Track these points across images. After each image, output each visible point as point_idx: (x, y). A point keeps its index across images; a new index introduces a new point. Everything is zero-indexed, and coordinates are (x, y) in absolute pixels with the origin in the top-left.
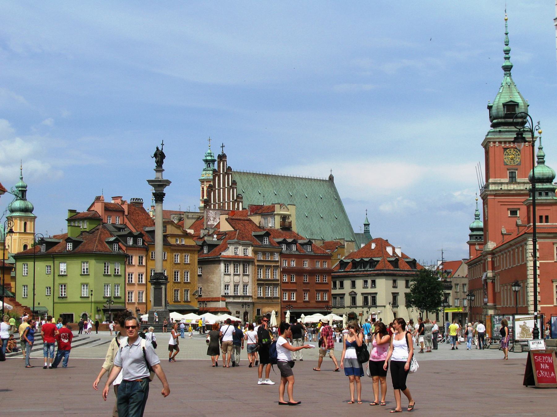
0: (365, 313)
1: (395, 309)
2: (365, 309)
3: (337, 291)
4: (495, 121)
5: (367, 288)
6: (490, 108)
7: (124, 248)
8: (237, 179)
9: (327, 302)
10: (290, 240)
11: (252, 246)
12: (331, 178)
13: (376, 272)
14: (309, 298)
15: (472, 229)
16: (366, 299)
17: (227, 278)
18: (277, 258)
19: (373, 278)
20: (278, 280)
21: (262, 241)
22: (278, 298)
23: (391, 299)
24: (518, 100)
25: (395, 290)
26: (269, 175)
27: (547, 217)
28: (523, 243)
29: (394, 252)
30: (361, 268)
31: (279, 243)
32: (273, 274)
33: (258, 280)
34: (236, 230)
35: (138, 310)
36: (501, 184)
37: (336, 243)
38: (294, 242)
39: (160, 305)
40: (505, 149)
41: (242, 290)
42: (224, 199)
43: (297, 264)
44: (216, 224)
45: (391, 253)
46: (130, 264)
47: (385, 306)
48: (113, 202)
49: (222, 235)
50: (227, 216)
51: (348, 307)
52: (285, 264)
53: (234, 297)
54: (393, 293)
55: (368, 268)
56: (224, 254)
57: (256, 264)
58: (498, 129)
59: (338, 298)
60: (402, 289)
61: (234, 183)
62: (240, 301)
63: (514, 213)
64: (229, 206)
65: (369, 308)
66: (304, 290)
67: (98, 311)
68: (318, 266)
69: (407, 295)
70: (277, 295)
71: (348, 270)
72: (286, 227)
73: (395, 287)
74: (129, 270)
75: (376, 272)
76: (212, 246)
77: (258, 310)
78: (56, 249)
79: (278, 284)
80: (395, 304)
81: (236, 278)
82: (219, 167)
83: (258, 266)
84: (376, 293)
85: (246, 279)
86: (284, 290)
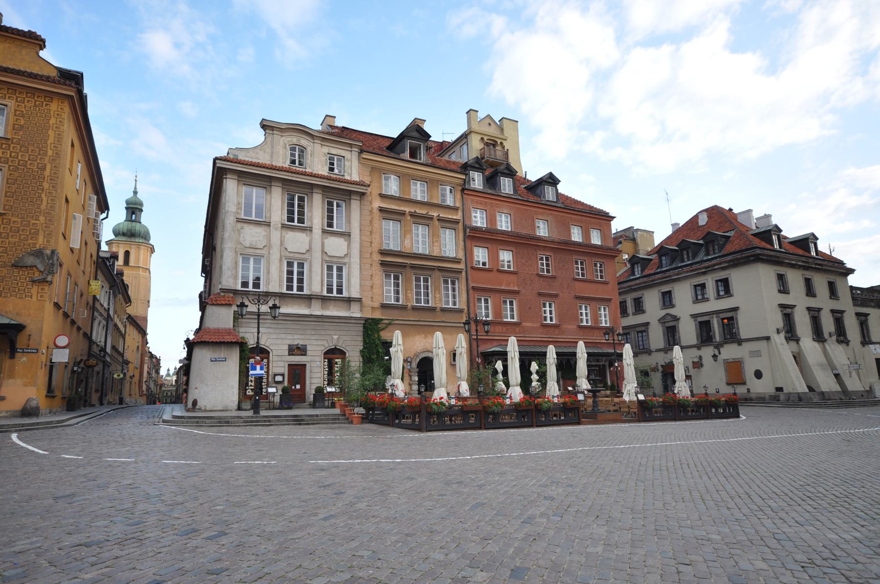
0: (707, 359)
1: (793, 344)
2: (707, 352)
5: (707, 300)
11: (361, 151)
13: (729, 258)
14: (560, 316)
17: (252, 235)
19: (722, 275)
20: (456, 261)
22: (460, 311)
23: (780, 324)
30: (683, 261)
32: (435, 237)
33: (383, 253)
41: (316, 279)
43: (514, 222)
47: (768, 338)
51: (658, 350)
52: (479, 219)
54: (782, 306)
55: (701, 256)
57: (377, 203)
62: (306, 311)
65: (718, 346)
66: (540, 294)
68: (576, 236)
69: (815, 315)
70: (461, 304)
71: (652, 272)
73: (780, 291)
75: (729, 258)
79: (459, 272)
83: (382, 210)
84: (735, 309)
85: (336, 246)
86: (473, 288)
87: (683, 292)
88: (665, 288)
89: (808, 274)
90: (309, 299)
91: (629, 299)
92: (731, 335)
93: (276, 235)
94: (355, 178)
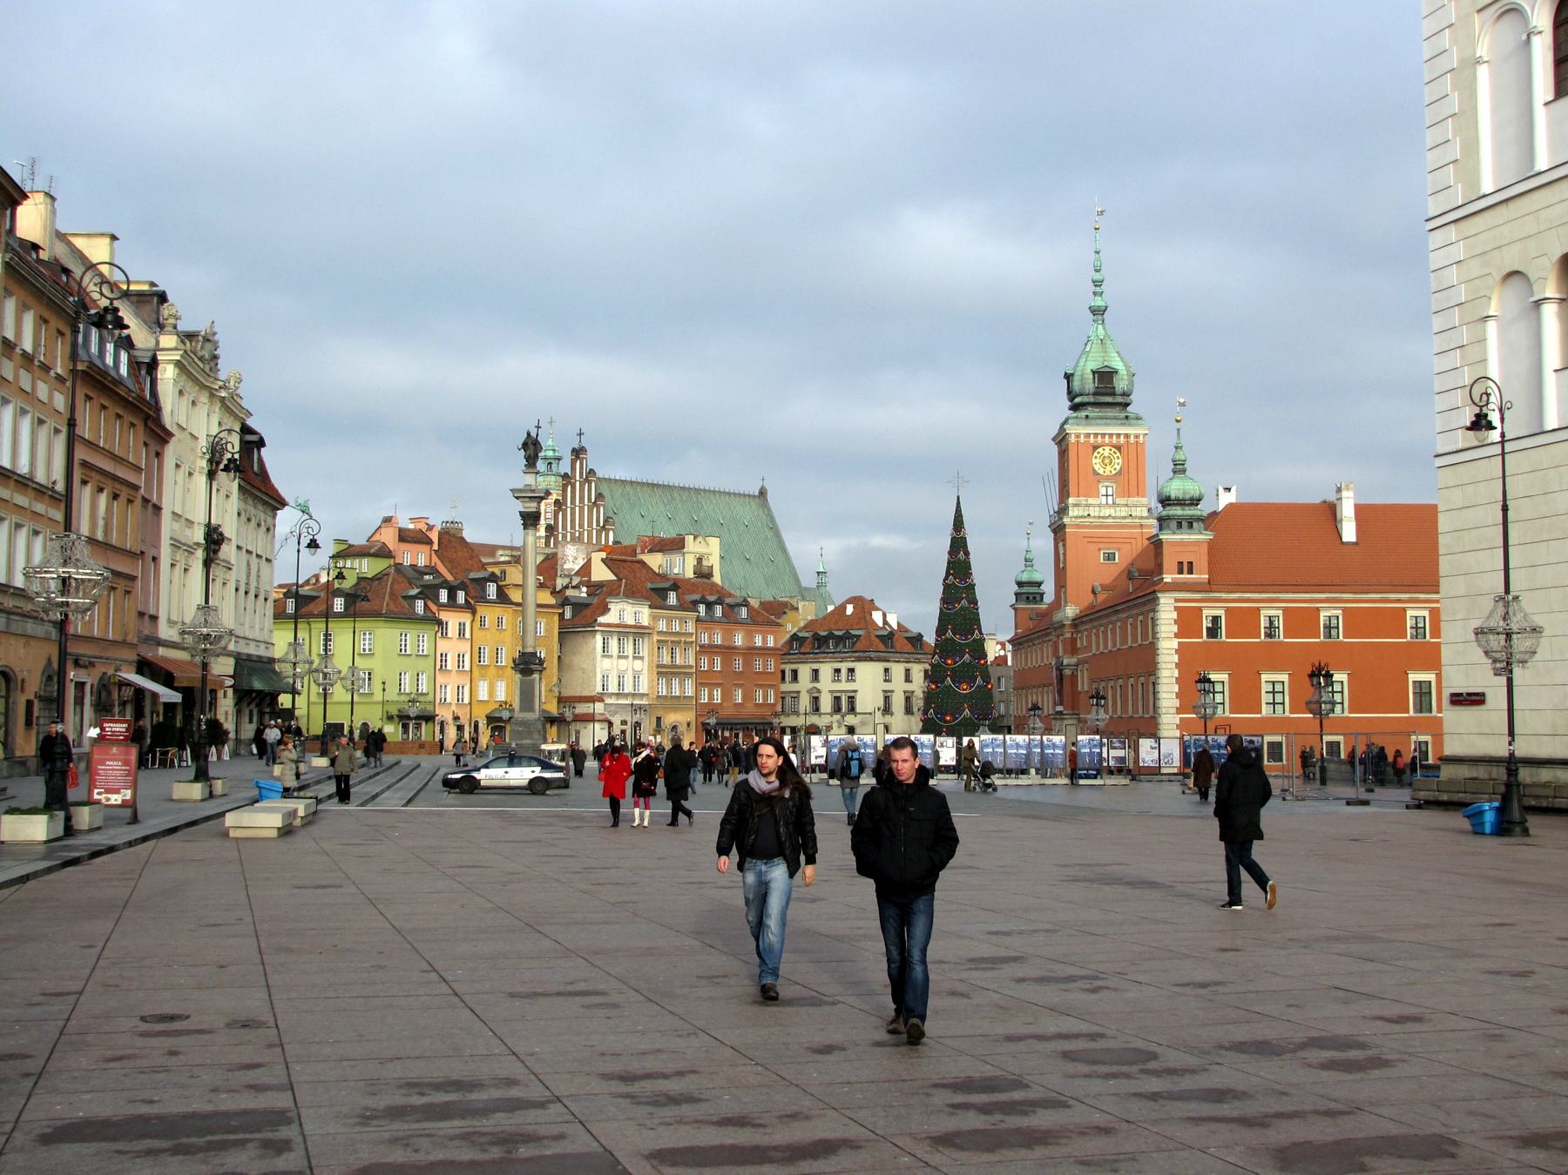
0: (835, 725)
2: (837, 717)
3: (788, 687)
4: (1077, 400)
6: (1068, 377)
7: (434, 608)
8: (605, 491)
9: (773, 705)
10: (712, 598)
12: (763, 493)
15: (1020, 584)
16: (837, 700)
17: (607, 661)
18: (691, 627)
19: (851, 665)
21: (665, 598)
23: (881, 704)
24: (1117, 364)
25: (887, 686)
26: (658, 485)
27: (1190, 564)
28: (1148, 607)
29: (885, 622)
31: (695, 603)
34: (620, 580)
35: (456, 718)
36: (1088, 506)
37: (785, 604)
38: (719, 602)
39: (531, 709)
40: (1095, 448)
42: (581, 526)
44: (577, 568)
45: (880, 624)
46: (444, 635)
48: (411, 526)
49: (596, 588)
50: (604, 555)
52: (705, 639)
53: (618, 695)
56: (601, 620)
57: (656, 638)
58: (1083, 414)
59: (788, 700)
60: (898, 686)
61: (600, 496)
63: (1110, 557)
64: (590, 537)
67: (390, 718)
68: (758, 642)
70: (690, 692)
72: (703, 573)
74: (443, 645)
76: (579, 607)
77: (659, 719)
78: (311, 607)
80: (887, 709)
81: (622, 661)
82: (573, 468)
85: (638, 665)
87: (826, 670)
88: (815, 666)
89: (908, 665)
90: (626, 695)
91: (788, 668)
92: (852, 710)
93: (615, 660)
94: (646, 623)
